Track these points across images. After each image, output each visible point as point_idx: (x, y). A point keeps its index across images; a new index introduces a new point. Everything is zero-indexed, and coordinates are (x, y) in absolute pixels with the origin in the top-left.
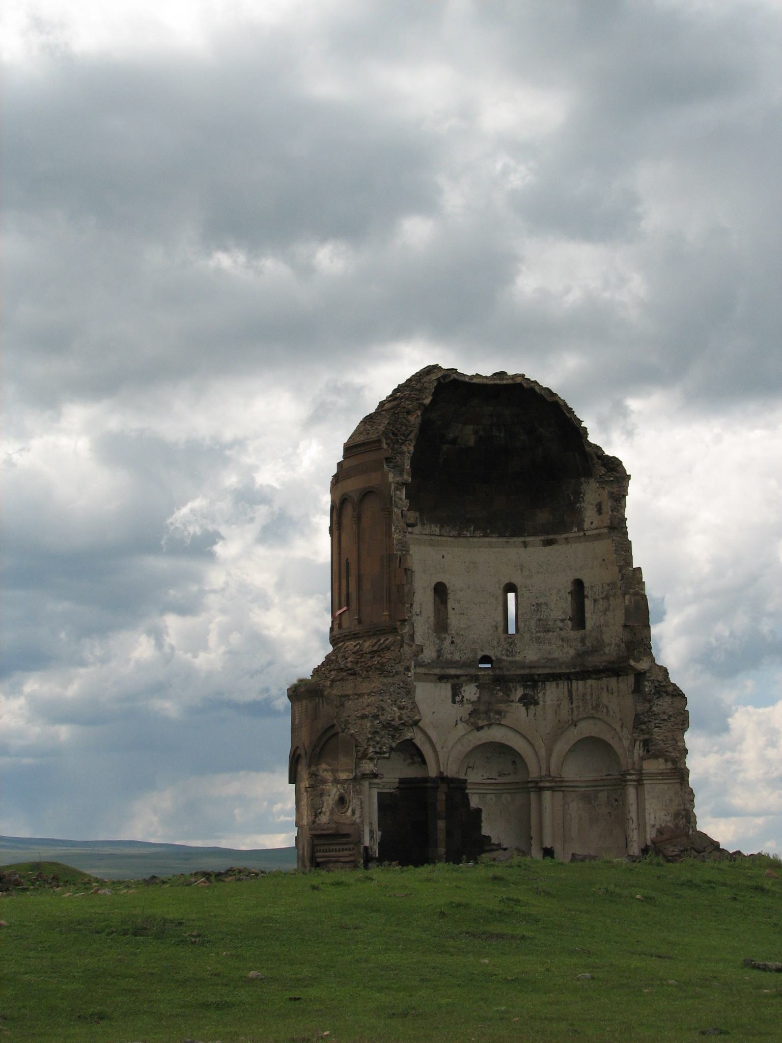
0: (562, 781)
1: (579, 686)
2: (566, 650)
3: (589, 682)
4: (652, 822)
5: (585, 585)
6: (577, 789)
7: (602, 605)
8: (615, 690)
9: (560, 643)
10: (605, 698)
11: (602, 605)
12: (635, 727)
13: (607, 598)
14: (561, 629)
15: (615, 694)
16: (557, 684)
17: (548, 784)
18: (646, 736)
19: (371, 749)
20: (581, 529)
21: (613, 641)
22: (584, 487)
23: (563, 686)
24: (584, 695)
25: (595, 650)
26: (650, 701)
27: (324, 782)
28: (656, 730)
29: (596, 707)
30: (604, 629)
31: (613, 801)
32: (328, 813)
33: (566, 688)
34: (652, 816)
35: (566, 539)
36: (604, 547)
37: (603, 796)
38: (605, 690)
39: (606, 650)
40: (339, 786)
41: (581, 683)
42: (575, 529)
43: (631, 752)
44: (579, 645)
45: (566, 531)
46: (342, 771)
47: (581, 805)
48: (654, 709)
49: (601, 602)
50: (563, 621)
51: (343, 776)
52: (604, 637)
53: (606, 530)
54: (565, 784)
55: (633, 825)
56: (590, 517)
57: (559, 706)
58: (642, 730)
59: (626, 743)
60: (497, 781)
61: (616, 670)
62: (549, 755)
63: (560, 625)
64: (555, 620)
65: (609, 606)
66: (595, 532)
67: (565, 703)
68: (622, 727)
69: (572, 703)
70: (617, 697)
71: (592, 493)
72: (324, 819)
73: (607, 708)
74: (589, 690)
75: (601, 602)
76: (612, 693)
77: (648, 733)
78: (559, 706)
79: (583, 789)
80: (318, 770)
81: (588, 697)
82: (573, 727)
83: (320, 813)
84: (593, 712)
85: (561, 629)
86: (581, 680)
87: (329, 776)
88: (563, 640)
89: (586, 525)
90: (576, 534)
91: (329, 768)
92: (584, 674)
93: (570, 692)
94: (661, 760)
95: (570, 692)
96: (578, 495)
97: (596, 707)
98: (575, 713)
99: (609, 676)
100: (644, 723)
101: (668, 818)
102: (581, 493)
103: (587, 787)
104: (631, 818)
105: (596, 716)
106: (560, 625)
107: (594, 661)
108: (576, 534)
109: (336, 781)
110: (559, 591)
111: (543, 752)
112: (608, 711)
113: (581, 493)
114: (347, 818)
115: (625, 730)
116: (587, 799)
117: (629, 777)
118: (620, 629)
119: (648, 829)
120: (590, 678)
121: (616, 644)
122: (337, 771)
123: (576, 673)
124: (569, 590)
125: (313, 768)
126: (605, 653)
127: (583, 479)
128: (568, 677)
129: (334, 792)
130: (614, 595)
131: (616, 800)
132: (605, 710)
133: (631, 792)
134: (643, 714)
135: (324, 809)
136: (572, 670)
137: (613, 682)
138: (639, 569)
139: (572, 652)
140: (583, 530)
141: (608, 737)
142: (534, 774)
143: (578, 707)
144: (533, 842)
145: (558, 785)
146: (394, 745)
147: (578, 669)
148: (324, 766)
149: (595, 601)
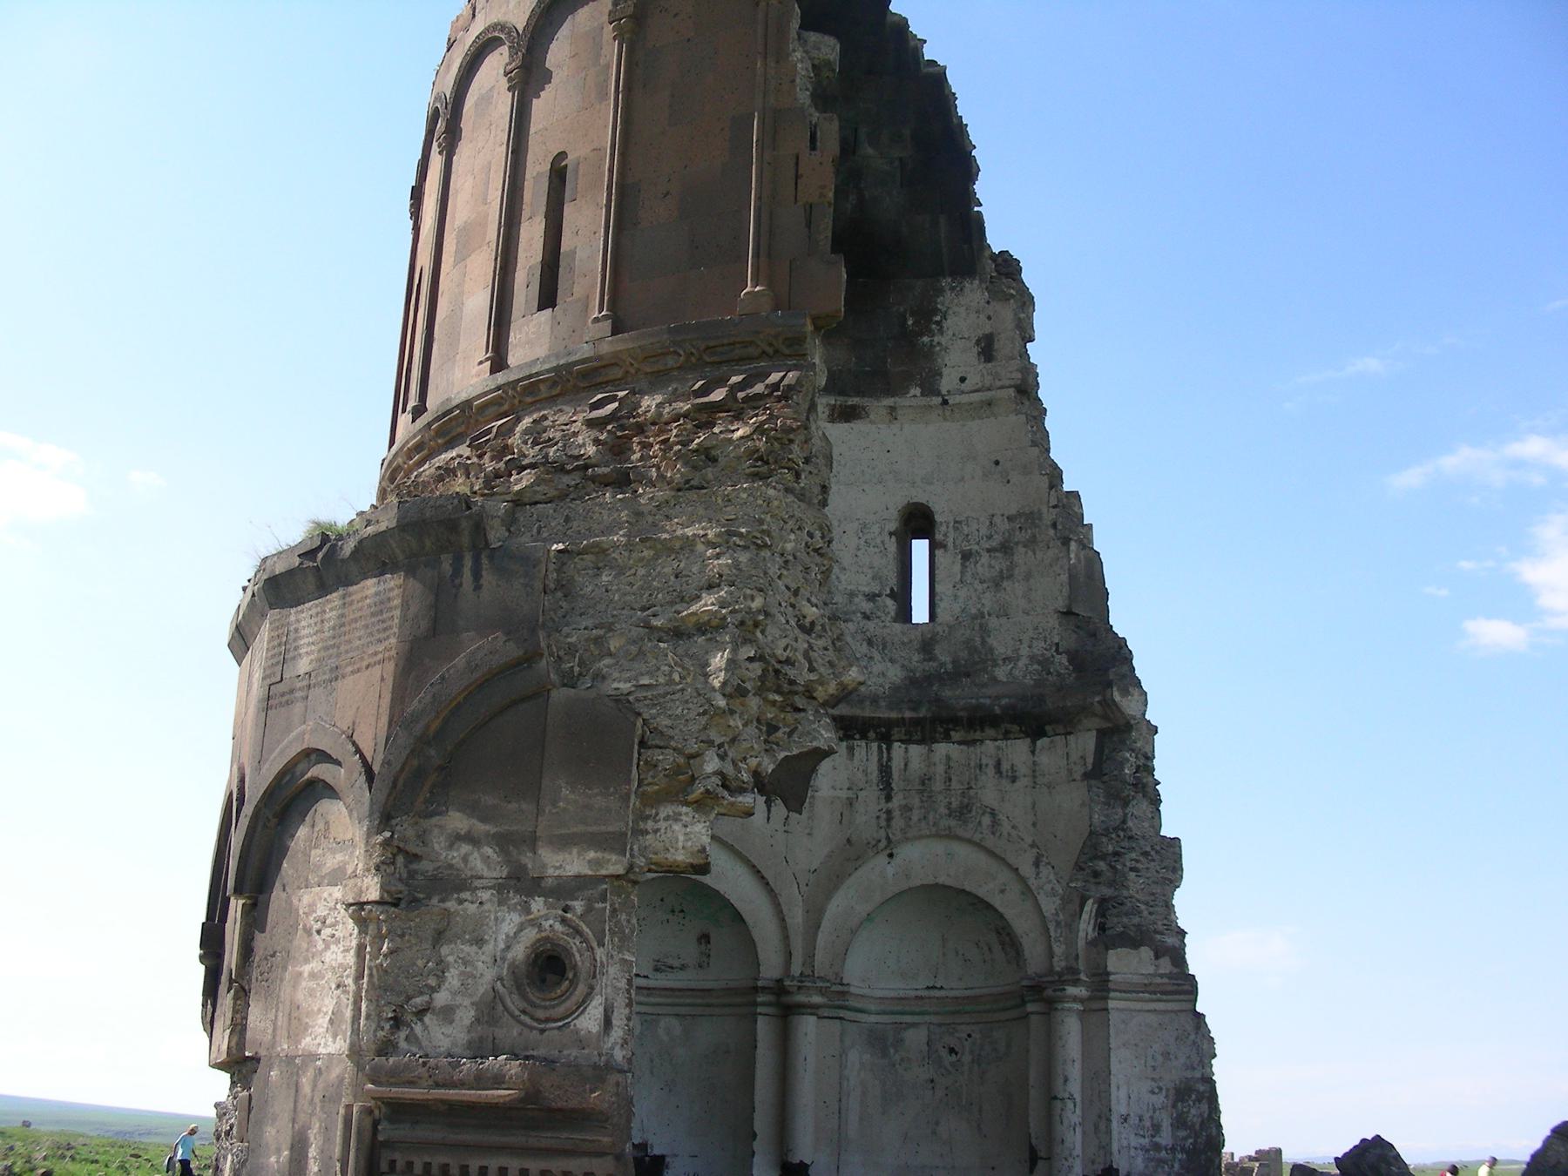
0: (843, 993)
1: (909, 757)
2: (877, 668)
3: (942, 749)
4: (1124, 1111)
5: (938, 518)
6: (859, 1017)
7: (986, 565)
8: (1022, 770)
9: (864, 648)
10: (988, 791)
11: (986, 565)
12: (1079, 868)
13: (1006, 548)
14: (866, 617)
15: (1023, 782)
16: (851, 750)
17: (817, 999)
18: (1107, 892)
19: (711, 764)
20: (930, 389)
21: (1024, 651)
22: (946, 300)
23: (867, 754)
24: (925, 780)
25: (960, 673)
26: (1126, 804)
27: (453, 883)
28: (1132, 875)
29: (962, 812)
30: (993, 622)
31: (944, 1053)
32: (466, 1016)
33: (874, 758)
34: (1123, 1094)
35: (892, 409)
36: (991, 433)
37: (916, 1038)
38: (991, 771)
39: (1001, 673)
40: (538, 905)
41: (916, 750)
42: (918, 391)
43: (1071, 926)
44: (916, 657)
45: (890, 392)
46: (564, 842)
47: (867, 1057)
48: (1130, 824)
49: (985, 559)
50: (872, 597)
51: (574, 864)
52: (990, 641)
53: (1012, 391)
54: (852, 1003)
55: (1073, 1115)
56: (956, 361)
57: (850, 803)
58: (1096, 874)
59: (1049, 906)
60: (651, 983)
61: (1031, 720)
62: (814, 926)
63: (867, 606)
64: (852, 595)
65: (1011, 567)
66: (976, 397)
67: (870, 799)
68: (1037, 864)
69: (889, 798)
70: (1033, 786)
71: (964, 312)
72: (442, 1036)
73: (993, 814)
74: (941, 769)
75: (985, 559)
76: (1014, 779)
77: (1111, 884)
78: (850, 803)
79: (873, 1019)
80: (423, 838)
81: (938, 785)
82: (882, 859)
83: (421, 1013)
84: (953, 823)
85: (866, 617)
86: (919, 742)
87: (483, 863)
88: (870, 643)
89: (947, 383)
90: (914, 402)
91: (482, 828)
92: (927, 730)
93: (885, 771)
94: (1146, 952)
95: (885, 771)
96: (928, 316)
97: (962, 812)
98: (898, 822)
99: (1007, 736)
100: (1103, 857)
101: (1159, 1100)
102: (936, 311)
103: (885, 1013)
104: (1071, 1098)
105: (960, 832)
106: (867, 606)
107: (959, 696)
108: (924, 401)
109: (521, 883)
110: (864, 527)
111: (796, 917)
112: (995, 823)
113: (936, 311)
114: (581, 1042)
115: (1045, 871)
116: (881, 1042)
117: (1072, 990)
118: (1054, 621)
119: (1115, 1124)
120: (947, 738)
121: (1032, 658)
122: (532, 841)
123: (917, 722)
124: (893, 526)
125: (405, 827)
126: (994, 680)
127: (945, 282)
128: (882, 732)
129: (510, 931)
130: (1032, 543)
131: (952, 1051)
132: (986, 820)
133: (1071, 1030)
134: (1106, 833)
135: (441, 998)
136: (908, 714)
137: (1017, 751)
138: (1075, 495)
139: (895, 674)
140: (938, 394)
141: (992, 886)
142: (771, 968)
143: (907, 809)
144: (756, 1145)
145: (839, 1001)
146: (769, 767)
147: (923, 713)
148: (457, 821)
149: (966, 556)
